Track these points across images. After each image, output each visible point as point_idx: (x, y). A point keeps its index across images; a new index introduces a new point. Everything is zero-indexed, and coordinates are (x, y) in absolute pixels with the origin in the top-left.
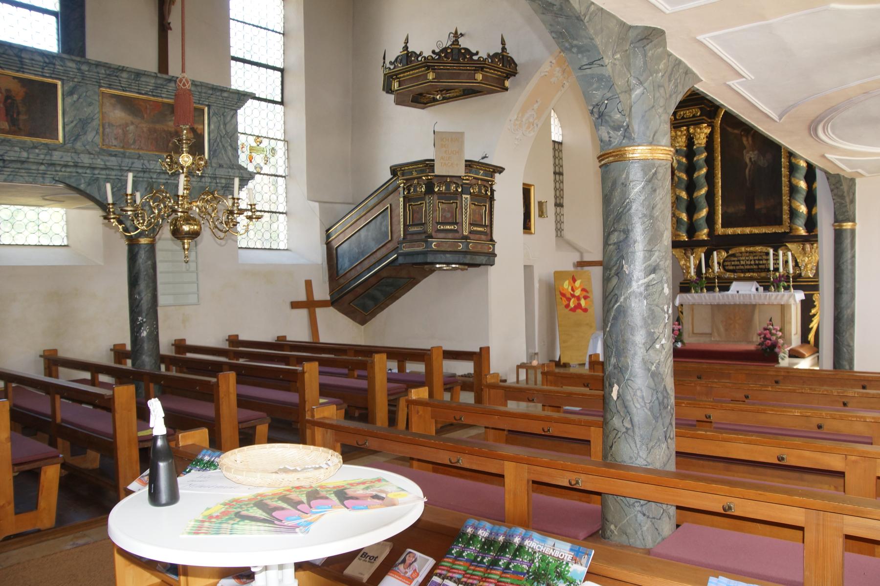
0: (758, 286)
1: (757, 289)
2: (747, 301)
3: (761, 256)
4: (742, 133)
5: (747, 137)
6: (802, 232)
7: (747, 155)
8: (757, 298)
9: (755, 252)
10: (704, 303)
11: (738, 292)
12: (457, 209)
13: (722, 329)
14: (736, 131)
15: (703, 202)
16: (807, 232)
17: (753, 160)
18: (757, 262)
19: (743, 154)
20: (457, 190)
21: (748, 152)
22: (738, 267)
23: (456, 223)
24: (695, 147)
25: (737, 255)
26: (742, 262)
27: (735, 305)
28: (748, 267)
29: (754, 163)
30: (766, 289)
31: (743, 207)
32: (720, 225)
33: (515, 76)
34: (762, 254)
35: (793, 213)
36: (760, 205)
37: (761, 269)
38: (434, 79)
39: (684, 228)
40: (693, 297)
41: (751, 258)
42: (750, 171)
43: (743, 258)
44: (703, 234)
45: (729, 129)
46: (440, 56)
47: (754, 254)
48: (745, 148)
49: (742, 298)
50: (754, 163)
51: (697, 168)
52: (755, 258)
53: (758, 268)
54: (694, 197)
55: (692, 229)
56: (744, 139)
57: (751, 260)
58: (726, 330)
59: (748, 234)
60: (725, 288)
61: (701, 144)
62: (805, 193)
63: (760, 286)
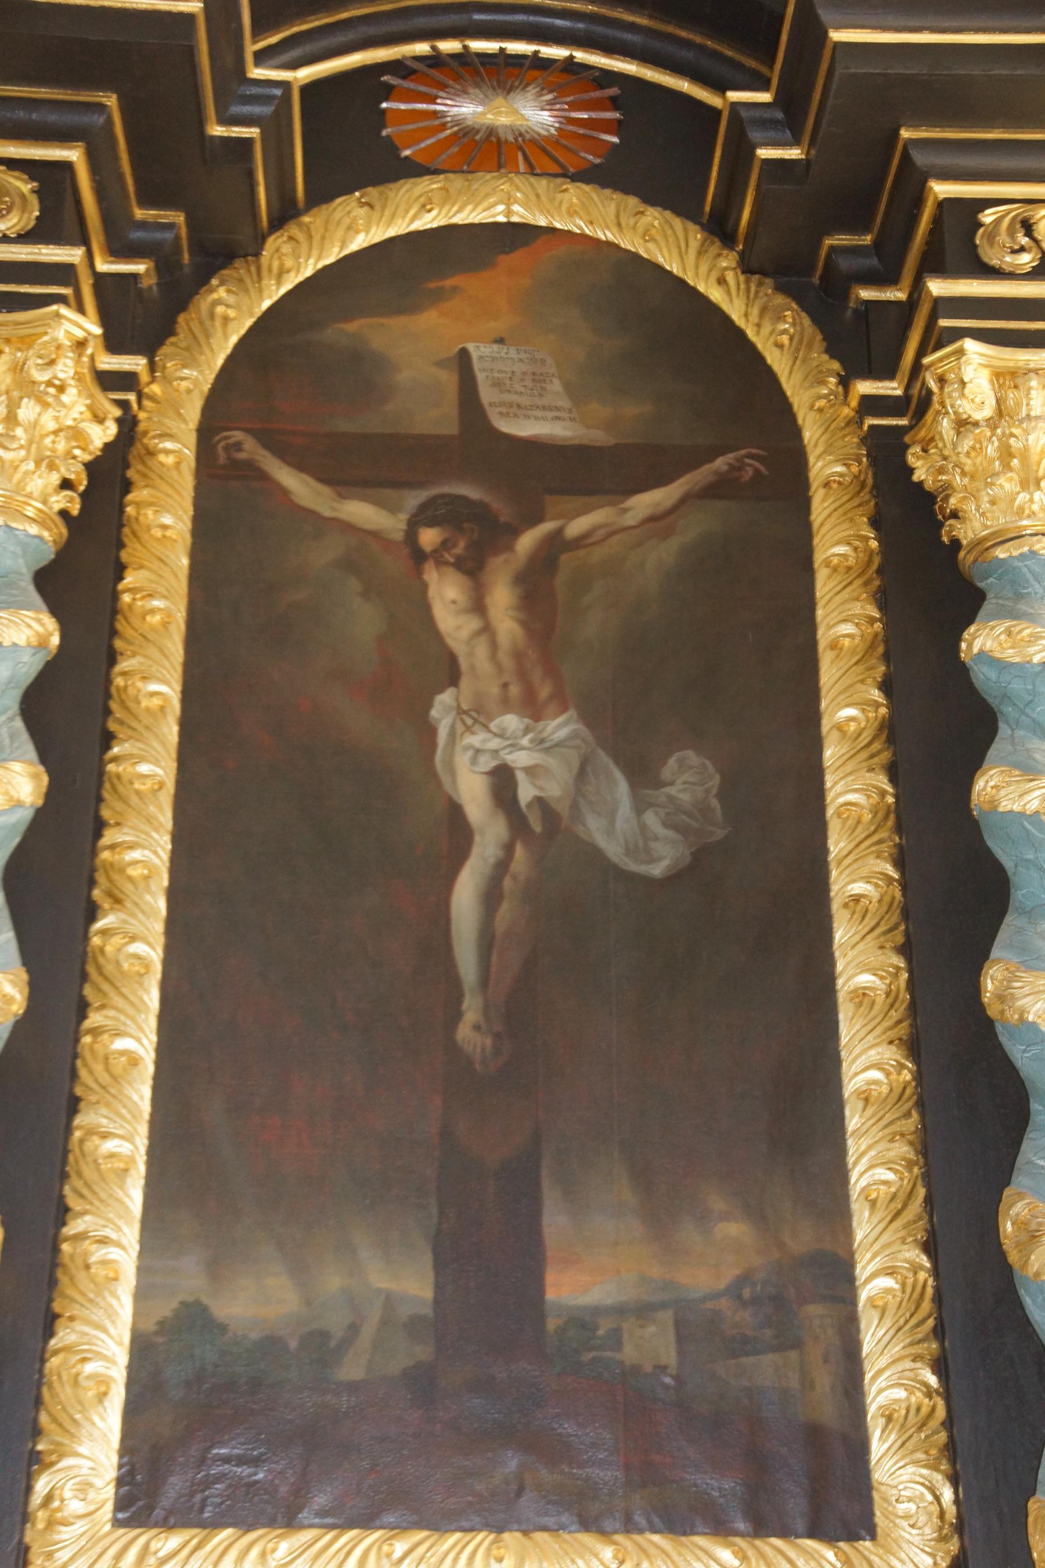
4: (429, 537)
7: (476, 739)
17: (526, 792)
19: (430, 732)
32: (106, 1492)
48: (452, 676)
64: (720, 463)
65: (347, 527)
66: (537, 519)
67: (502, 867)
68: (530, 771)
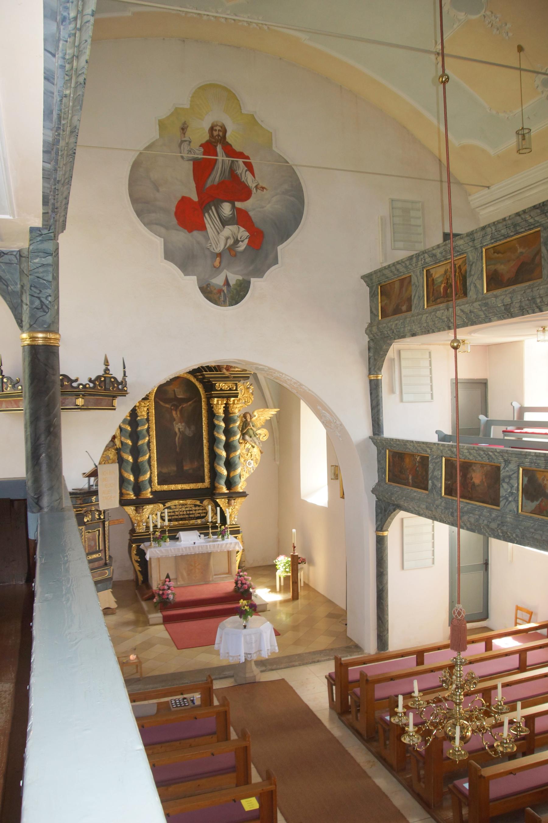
0: (199, 534)
1: (200, 536)
2: (205, 551)
3: (191, 507)
4: (172, 408)
5: (176, 410)
6: (225, 490)
7: (177, 426)
8: (212, 547)
9: (186, 505)
10: (170, 556)
11: (194, 543)
12: (101, 536)
13: (185, 574)
14: (167, 406)
15: (147, 466)
16: (227, 490)
17: (181, 430)
18: (188, 512)
19: (173, 425)
20: (100, 518)
21: (177, 424)
22: (173, 517)
23: (99, 551)
24: (139, 418)
25: (172, 507)
26: (177, 513)
27: (195, 555)
28: (182, 517)
29: (182, 433)
30: (206, 534)
31: (174, 468)
33: (125, 396)
34: (192, 506)
35: (214, 475)
36: (187, 467)
37: (192, 517)
38: (83, 406)
39: (131, 487)
40: (160, 551)
41: (184, 509)
42: (179, 439)
43: (177, 510)
44: (148, 494)
45: (161, 403)
46: (95, 384)
47: (186, 506)
49: (200, 548)
50: (182, 433)
51: (140, 438)
52: (187, 509)
53: (189, 517)
54: (139, 461)
55: (138, 488)
56: (174, 413)
57: (183, 511)
58: (188, 575)
59: (179, 490)
60: (174, 538)
61: (143, 416)
62: (224, 460)
63: (201, 533)
64: (195, 399)
65: (166, 407)
66: (180, 405)
67: (179, 436)
68: (181, 428)
